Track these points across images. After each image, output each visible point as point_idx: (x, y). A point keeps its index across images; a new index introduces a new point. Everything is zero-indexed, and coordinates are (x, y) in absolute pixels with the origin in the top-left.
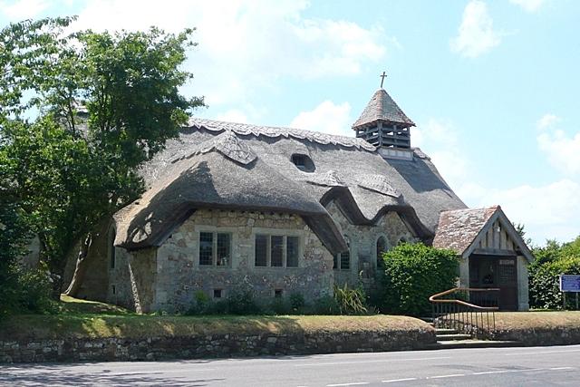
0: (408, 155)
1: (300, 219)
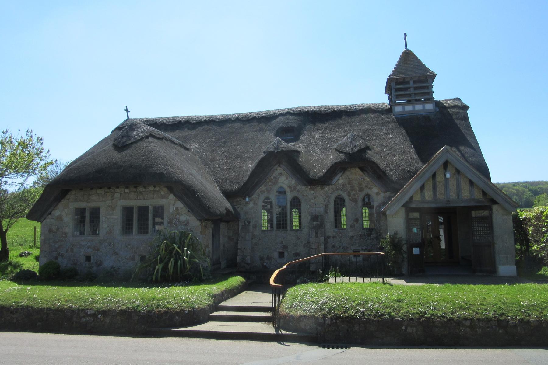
0: (429, 107)
1: (165, 189)
